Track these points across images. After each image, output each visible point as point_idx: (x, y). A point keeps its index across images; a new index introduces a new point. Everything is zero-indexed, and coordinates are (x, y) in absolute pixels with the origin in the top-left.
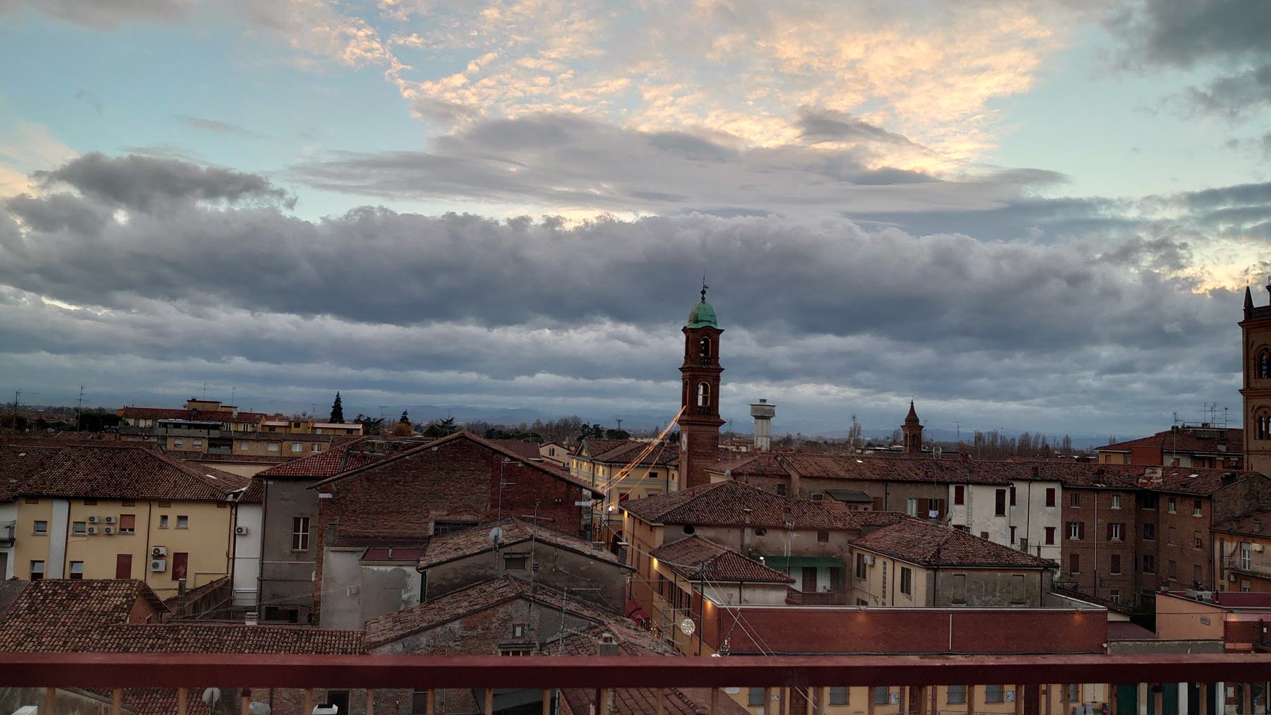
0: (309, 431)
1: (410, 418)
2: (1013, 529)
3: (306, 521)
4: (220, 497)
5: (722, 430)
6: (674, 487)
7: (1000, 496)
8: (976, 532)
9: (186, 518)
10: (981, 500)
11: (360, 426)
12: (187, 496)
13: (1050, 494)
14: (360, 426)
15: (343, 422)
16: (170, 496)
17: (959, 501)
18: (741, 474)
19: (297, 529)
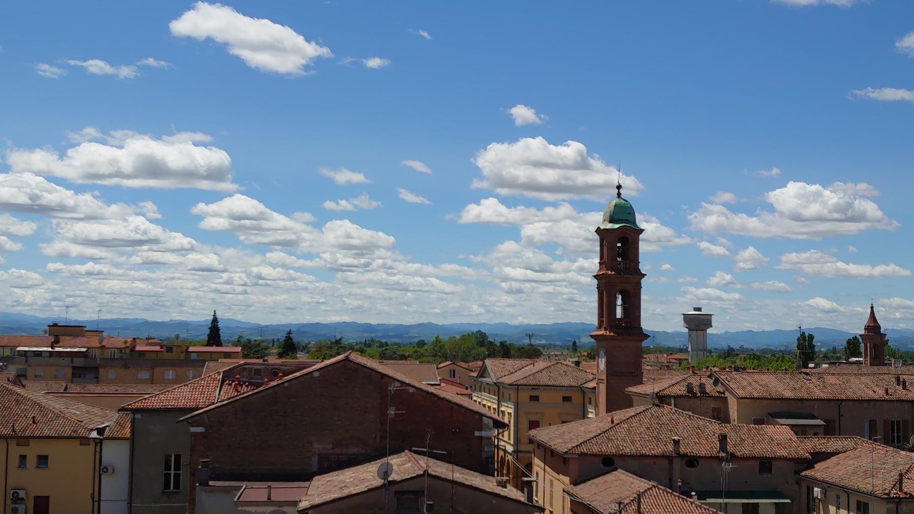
0: (183, 356)
1: (296, 338)
3: (177, 458)
4: (82, 432)
9: (46, 457)
11: (239, 349)
12: (46, 432)
15: (219, 344)
16: (28, 433)
18: (669, 396)
19: (168, 467)
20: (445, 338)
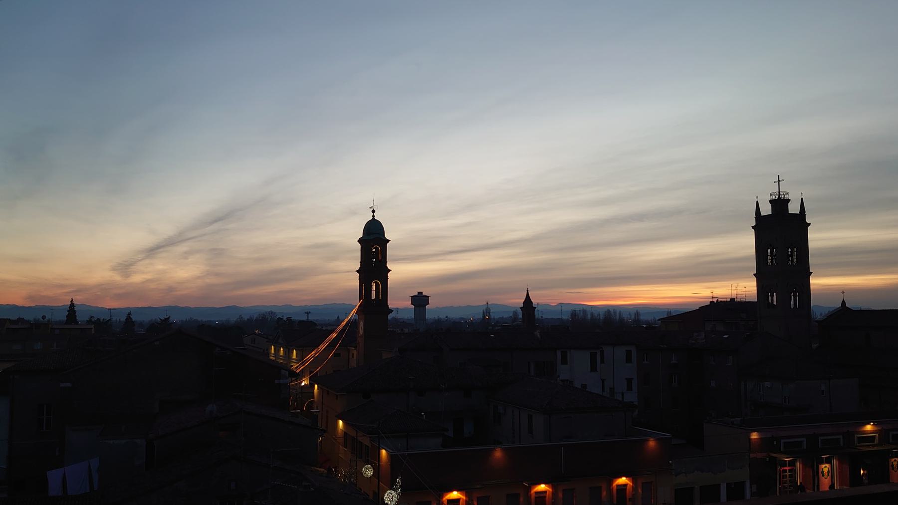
2: (603, 381)
5: (390, 316)
6: (353, 364)
7: (593, 357)
8: (577, 385)
10: (580, 360)
11: (93, 326)
13: (629, 353)
14: (93, 326)
17: (564, 361)
20: (246, 318)
